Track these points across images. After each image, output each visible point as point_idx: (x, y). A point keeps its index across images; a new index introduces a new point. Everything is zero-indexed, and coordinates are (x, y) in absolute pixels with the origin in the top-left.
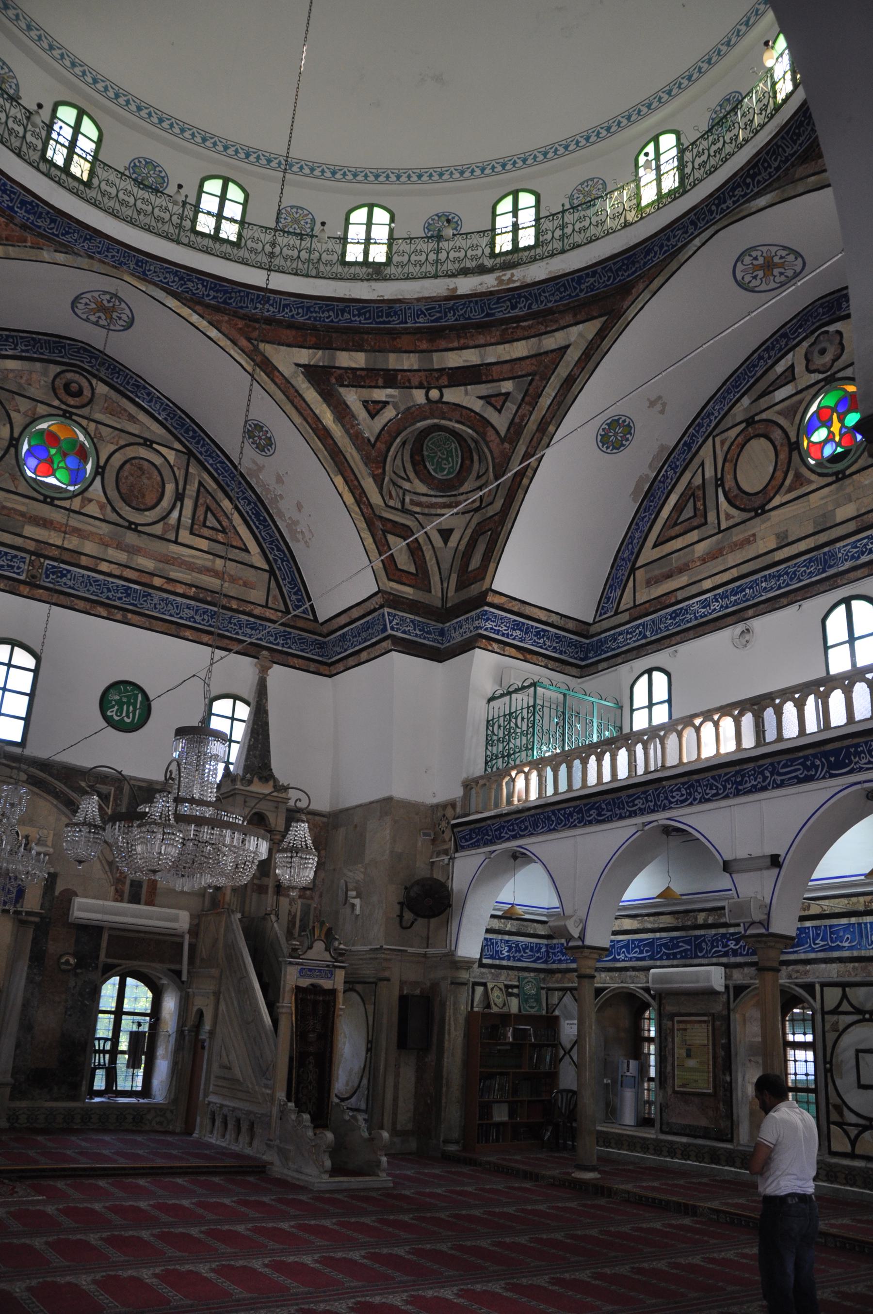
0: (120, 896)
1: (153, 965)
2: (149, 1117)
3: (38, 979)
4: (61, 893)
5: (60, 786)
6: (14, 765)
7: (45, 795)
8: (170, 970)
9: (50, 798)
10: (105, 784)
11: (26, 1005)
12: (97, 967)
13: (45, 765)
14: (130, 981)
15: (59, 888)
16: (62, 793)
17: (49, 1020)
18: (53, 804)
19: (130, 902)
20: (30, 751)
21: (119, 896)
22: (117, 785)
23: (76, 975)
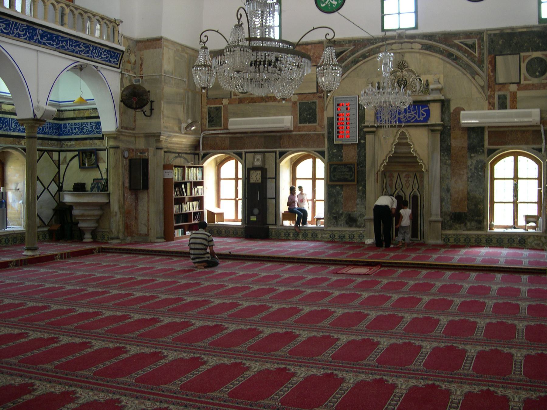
0: (492, 106)
1: (521, 146)
2: (530, 240)
3: (449, 162)
4: (455, 110)
5: (442, 46)
6: (412, 41)
7: (434, 54)
8: (533, 149)
9: (438, 55)
10: (470, 38)
11: (442, 179)
12: (483, 152)
13: (430, 36)
14: (520, 158)
15: (452, 108)
16: (444, 50)
17: (460, 185)
18: (439, 58)
19: (499, 109)
20: (422, 30)
21: (492, 106)
22: (479, 37)
23: (471, 157)
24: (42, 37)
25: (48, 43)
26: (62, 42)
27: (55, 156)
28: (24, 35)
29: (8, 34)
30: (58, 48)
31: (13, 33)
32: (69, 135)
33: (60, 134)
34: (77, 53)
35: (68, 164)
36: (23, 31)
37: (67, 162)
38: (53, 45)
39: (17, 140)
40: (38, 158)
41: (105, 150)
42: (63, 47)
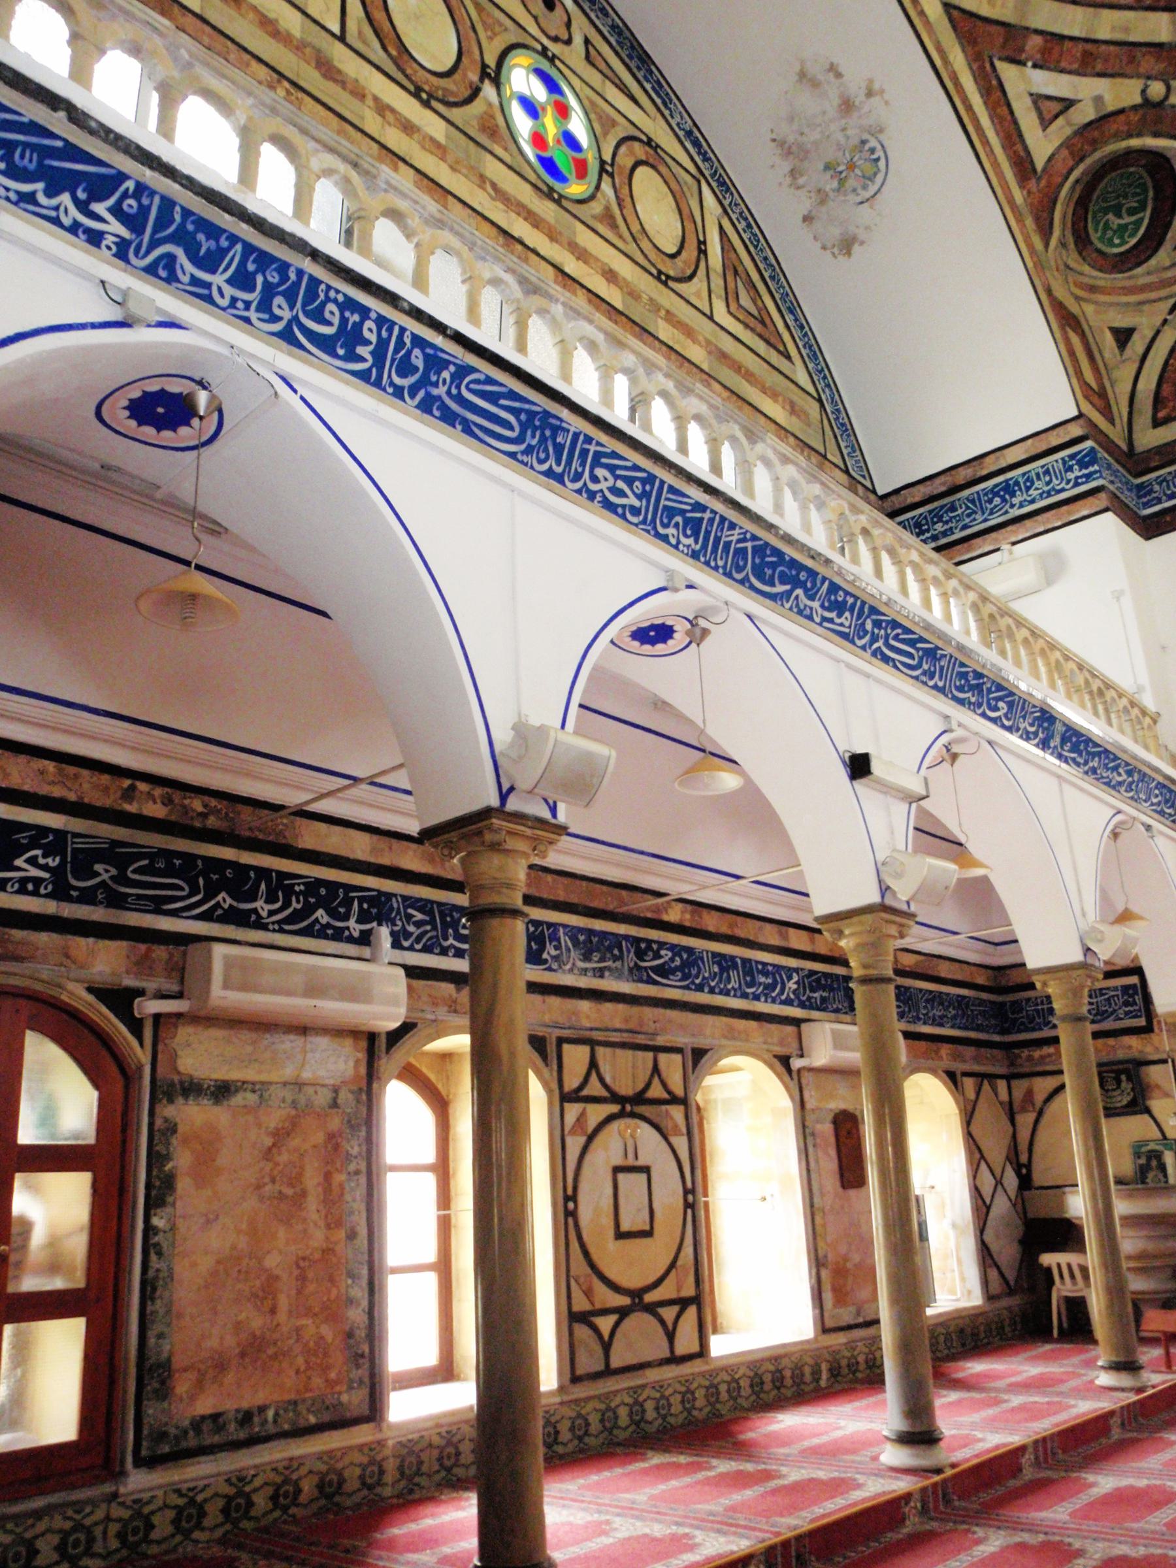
24: (1064, 740)
25: (1074, 760)
26: (1094, 755)
27: (1002, 1085)
28: (1036, 734)
29: (1009, 729)
30: (1086, 773)
31: (1018, 730)
32: (1033, 1030)
33: (1003, 1032)
34: (1114, 788)
35: (1040, 1113)
36: (1032, 725)
37: (1038, 1104)
38: (1078, 764)
39: (933, 1046)
40: (972, 1096)
41: (1164, 1061)
42: (1094, 771)
